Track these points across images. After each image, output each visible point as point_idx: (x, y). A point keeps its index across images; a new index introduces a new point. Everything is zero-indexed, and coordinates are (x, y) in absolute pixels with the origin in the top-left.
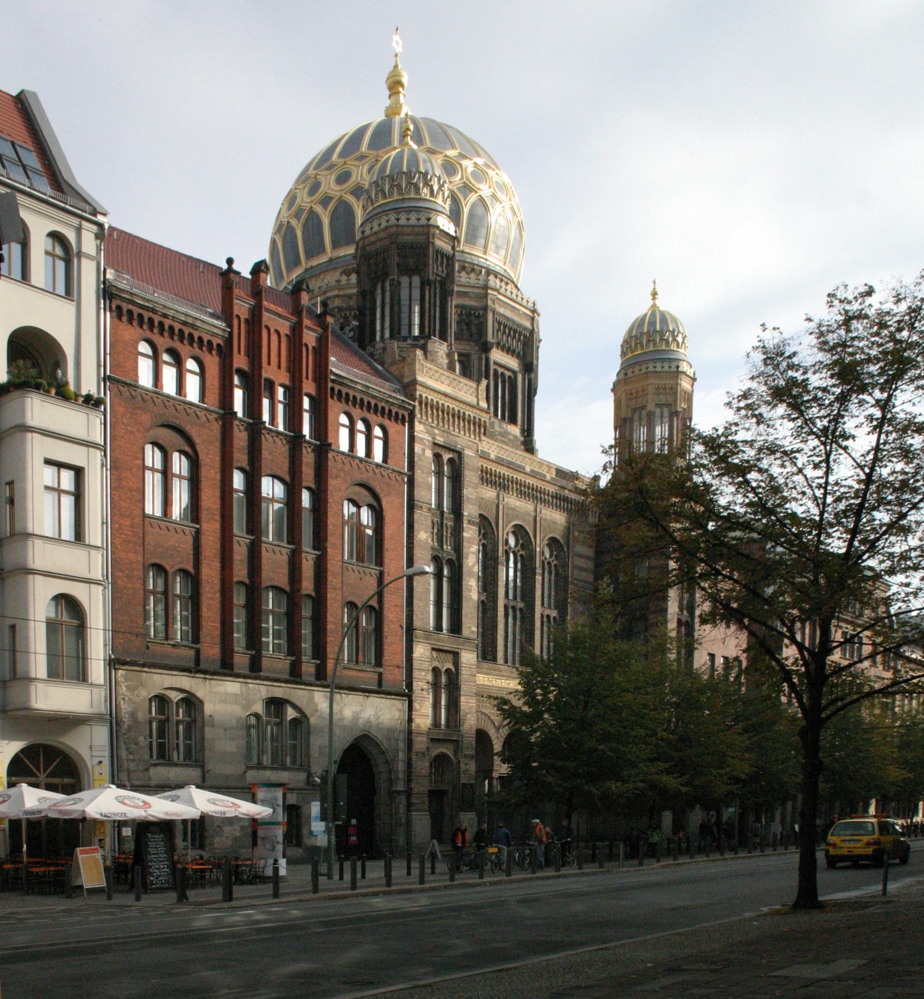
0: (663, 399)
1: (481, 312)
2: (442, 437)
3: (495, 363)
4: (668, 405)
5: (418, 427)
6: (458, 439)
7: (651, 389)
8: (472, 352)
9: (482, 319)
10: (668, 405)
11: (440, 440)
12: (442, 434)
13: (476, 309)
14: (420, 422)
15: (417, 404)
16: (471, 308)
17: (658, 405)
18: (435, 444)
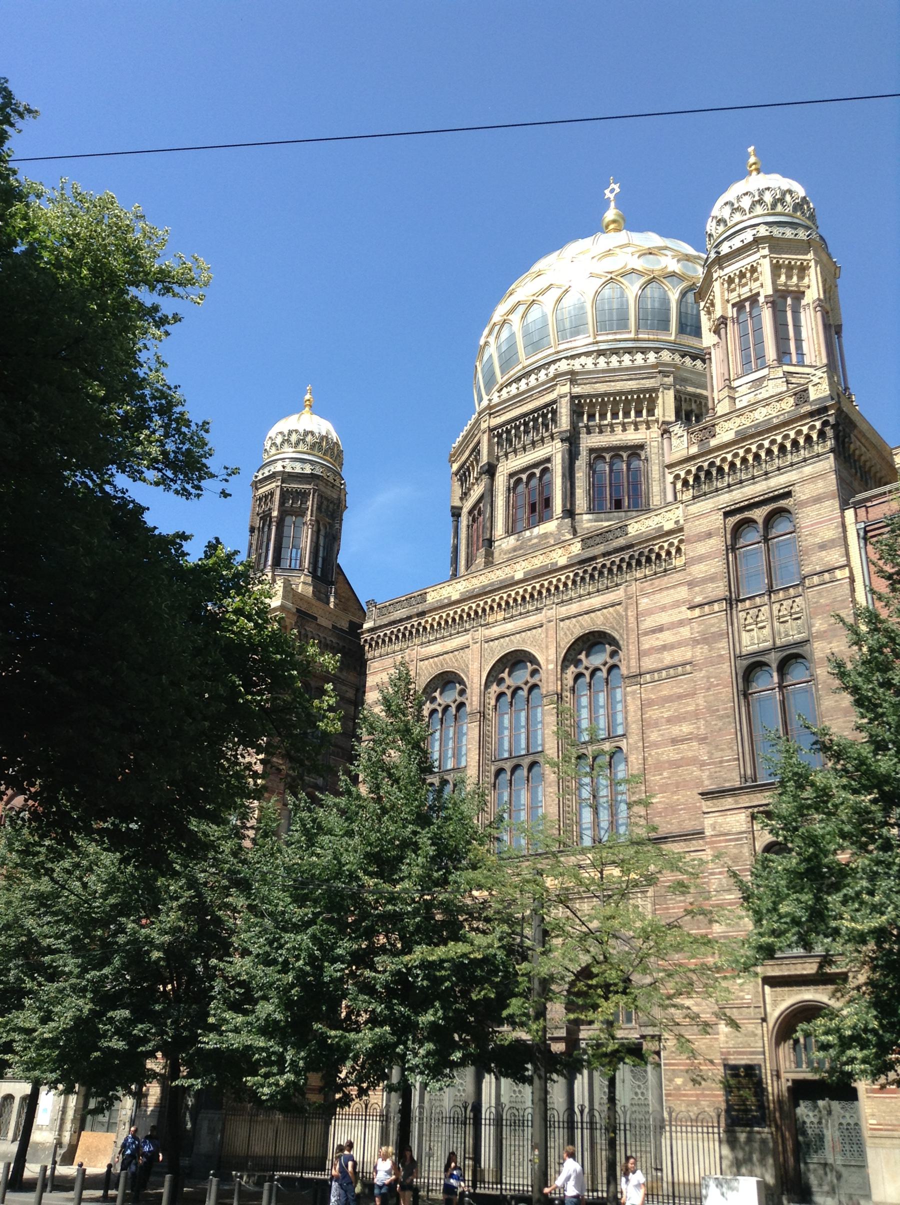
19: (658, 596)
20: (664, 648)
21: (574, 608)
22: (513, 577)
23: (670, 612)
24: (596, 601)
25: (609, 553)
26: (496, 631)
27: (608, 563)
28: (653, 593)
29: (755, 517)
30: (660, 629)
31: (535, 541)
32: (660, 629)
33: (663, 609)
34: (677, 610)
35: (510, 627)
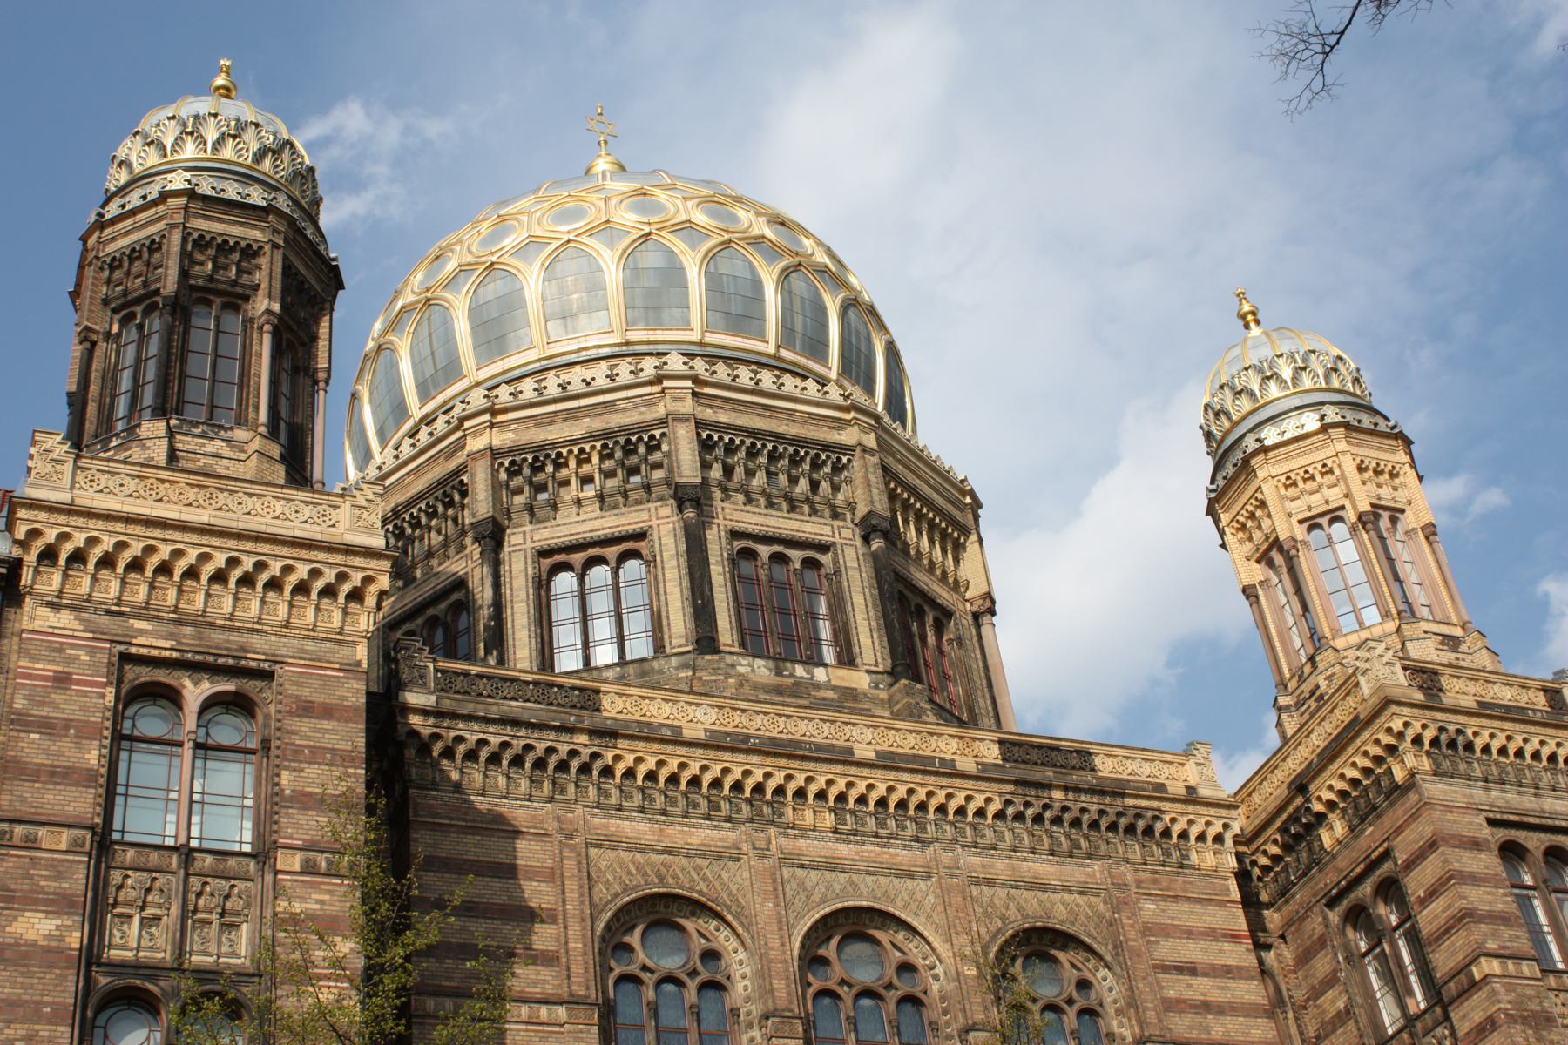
0: (1317, 503)
1: (657, 433)
2: (171, 636)
3: (735, 535)
4: (1335, 516)
5: (35, 618)
6: (255, 640)
7: (1269, 492)
8: (654, 522)
9: (665, 447)
10: (1335, 516)
11: (151, 639)
12: (165, 628)
13: (640, 428)
14: (55, 606)
15: (31, 558)
16: (627, 430)
17: (1312, 524)
18: (126, 658)
19: (1173, 907)
20: (1206, 1007)
21: (1000, 866)
22: (850, 751)
23: (1202, 945)
24: (1045, 868)
25: (1077, 790)
26: (813, 848)
27: (1076, 807)
28: (1164, 898)
29: (1529, 845)
30: (1192, 970)
31: (830, 694)
32: (1192, 970)
33: (1189, 933)
34: (1215, 946)
35: (845, 850)
